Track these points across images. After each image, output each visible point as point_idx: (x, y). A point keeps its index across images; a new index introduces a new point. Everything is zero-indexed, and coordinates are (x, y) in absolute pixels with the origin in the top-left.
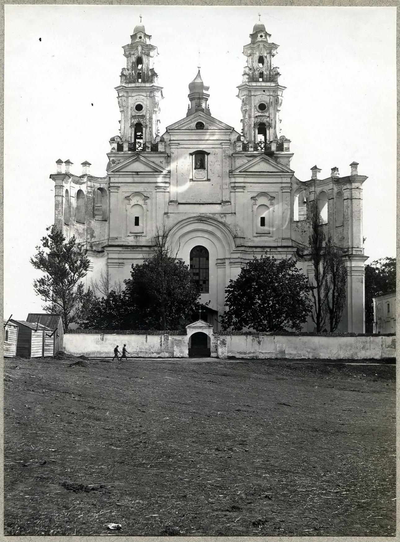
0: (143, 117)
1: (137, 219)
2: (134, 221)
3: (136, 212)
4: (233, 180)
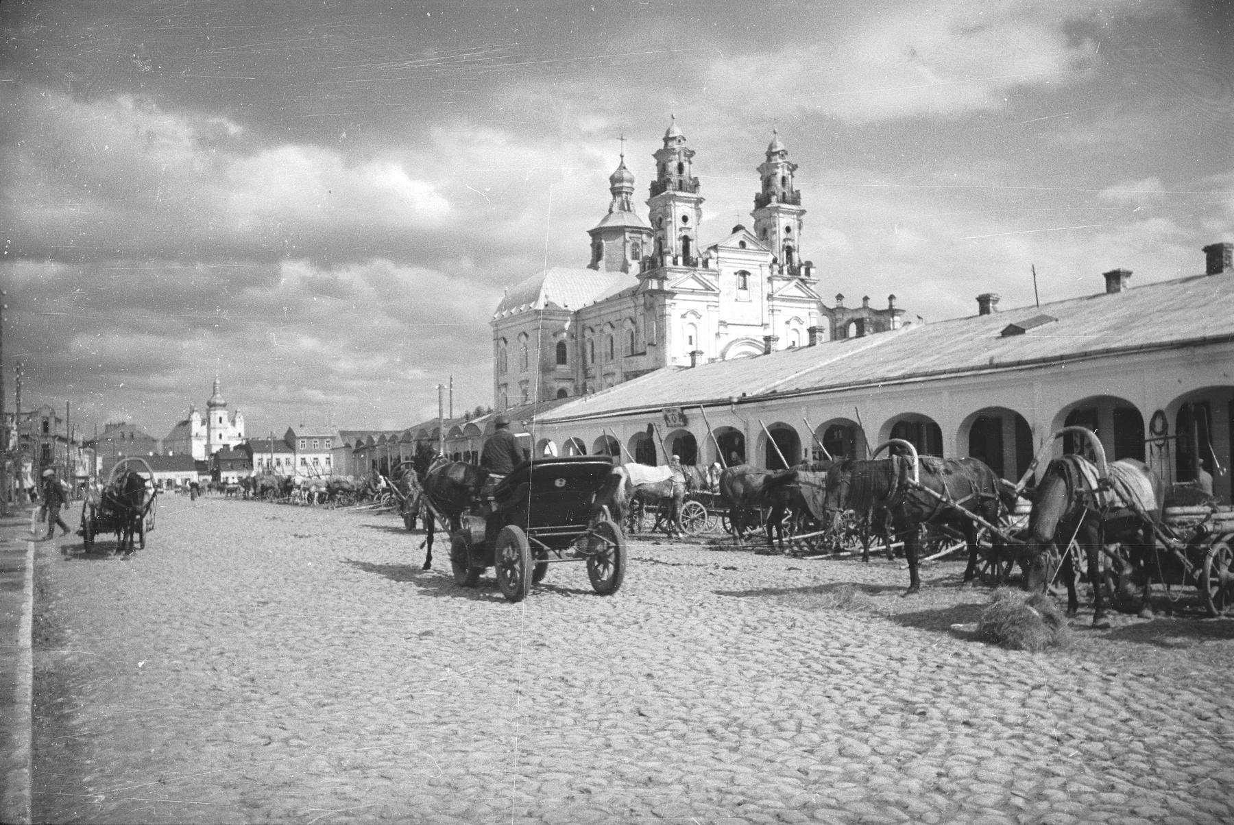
0: (689, 229)
1: (691, 337)
2: (688, 339)
3: (691, 331)
4: (771, 303)
